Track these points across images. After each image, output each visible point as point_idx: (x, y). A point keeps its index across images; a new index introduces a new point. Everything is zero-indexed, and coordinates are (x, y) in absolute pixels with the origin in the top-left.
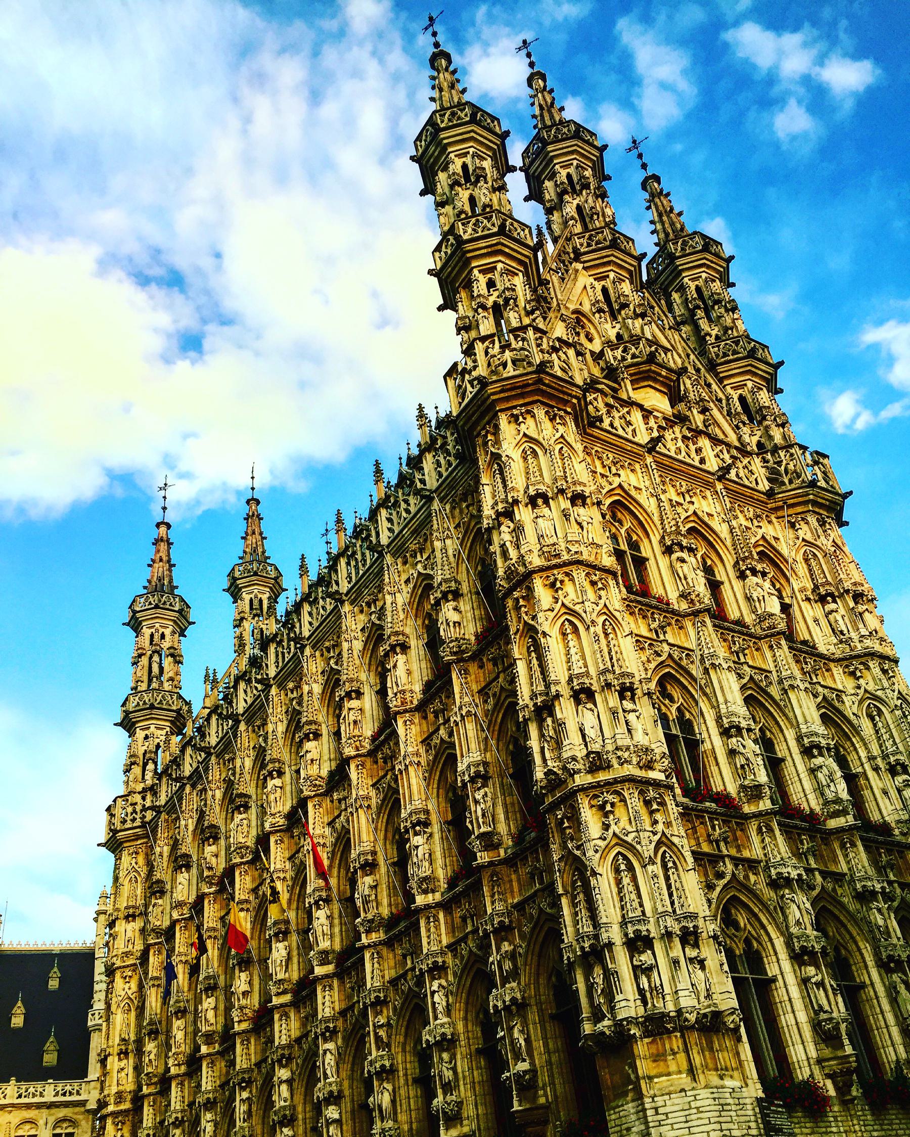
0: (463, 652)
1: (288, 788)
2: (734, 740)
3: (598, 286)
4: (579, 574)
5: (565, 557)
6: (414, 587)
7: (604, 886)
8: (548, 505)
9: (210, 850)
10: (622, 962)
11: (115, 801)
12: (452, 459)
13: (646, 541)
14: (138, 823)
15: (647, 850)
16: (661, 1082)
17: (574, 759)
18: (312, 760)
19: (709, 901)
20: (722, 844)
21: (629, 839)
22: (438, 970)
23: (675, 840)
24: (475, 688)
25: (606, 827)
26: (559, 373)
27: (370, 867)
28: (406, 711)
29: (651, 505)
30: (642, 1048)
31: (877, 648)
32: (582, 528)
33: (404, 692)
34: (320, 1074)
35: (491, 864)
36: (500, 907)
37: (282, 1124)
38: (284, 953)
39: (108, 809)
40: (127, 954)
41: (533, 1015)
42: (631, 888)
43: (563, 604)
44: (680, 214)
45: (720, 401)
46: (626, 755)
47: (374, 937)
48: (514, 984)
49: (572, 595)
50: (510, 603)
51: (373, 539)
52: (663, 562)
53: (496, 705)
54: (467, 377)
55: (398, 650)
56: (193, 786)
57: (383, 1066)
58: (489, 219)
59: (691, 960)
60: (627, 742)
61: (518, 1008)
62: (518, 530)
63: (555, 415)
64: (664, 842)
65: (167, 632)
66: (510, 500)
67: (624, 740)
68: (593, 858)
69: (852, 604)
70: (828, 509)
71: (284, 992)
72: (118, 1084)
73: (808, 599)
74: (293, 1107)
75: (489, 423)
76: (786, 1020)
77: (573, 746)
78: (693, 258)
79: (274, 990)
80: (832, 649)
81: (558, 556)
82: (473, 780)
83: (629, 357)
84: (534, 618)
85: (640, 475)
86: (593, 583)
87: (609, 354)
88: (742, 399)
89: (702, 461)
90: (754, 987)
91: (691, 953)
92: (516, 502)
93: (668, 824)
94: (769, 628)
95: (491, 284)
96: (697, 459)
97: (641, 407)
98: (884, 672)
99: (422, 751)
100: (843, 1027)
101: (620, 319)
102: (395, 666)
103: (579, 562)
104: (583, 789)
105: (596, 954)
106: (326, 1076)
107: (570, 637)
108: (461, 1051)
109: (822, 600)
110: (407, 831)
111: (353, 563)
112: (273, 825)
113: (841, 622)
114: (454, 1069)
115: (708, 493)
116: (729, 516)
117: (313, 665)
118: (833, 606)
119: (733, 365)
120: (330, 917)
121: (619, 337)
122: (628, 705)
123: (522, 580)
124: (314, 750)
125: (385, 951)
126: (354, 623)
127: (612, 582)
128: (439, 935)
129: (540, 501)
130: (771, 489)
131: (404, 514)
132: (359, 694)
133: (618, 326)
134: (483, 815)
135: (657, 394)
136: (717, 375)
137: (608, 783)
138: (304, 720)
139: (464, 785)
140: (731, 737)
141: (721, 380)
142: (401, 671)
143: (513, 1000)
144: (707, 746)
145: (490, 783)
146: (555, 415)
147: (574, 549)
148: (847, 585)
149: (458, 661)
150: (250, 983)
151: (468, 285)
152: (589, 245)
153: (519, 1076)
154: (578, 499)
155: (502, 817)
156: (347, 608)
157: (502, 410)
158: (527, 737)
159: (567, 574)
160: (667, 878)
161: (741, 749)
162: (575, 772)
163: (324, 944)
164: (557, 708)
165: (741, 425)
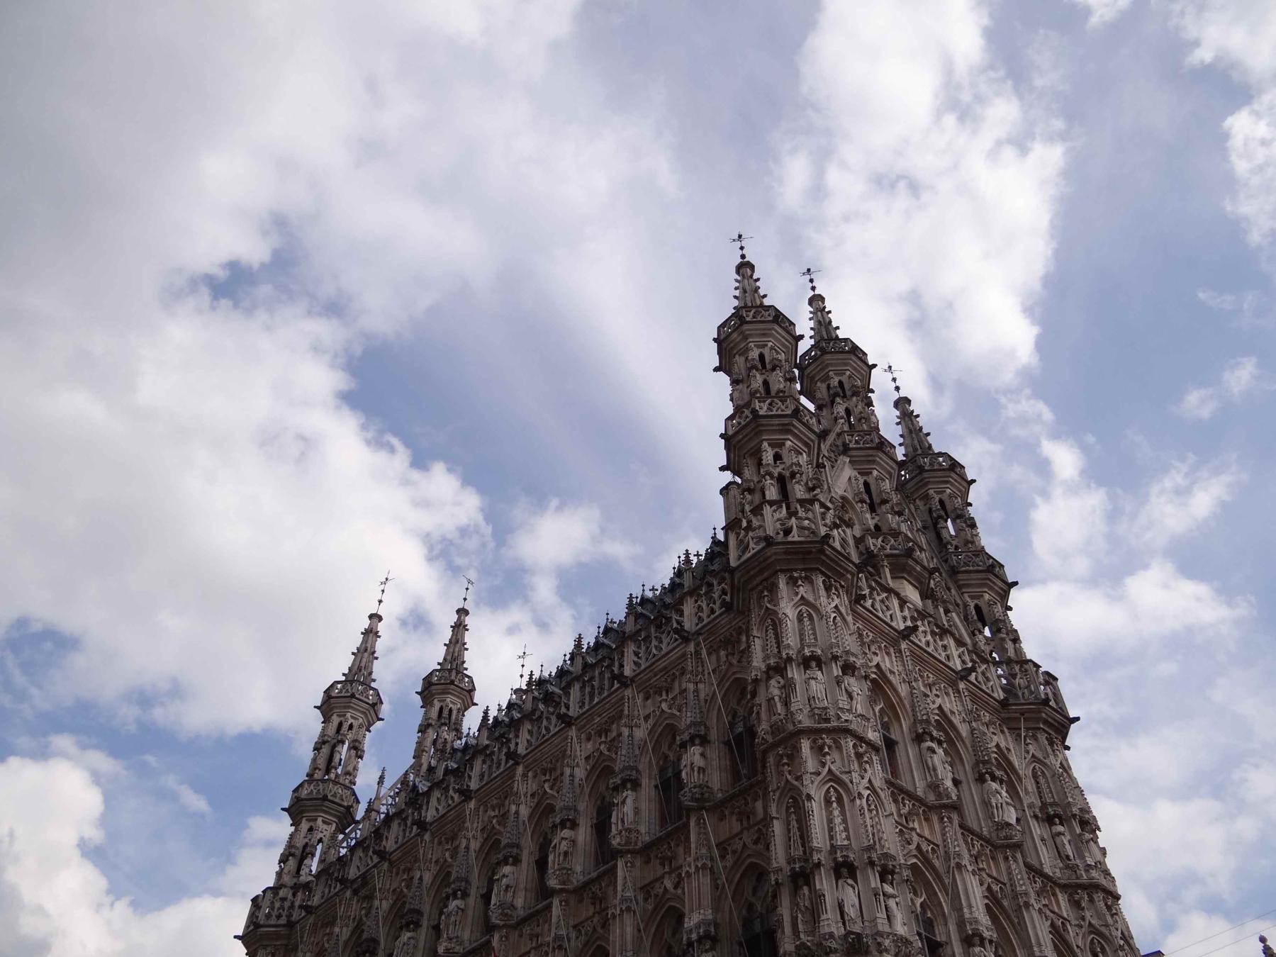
1: (470, 913)
2: (977, 949)
3: (861, 481)
4: (849, 743)
5: (834, 724)
6: (655, 725)
8: (821, 669)
11: (264, 892)
12: (716, 607)
13: (896, 725)
14: (283, 921)
17: (831, 935)
18: (507, 887)
26: (839, 548)
28: (628, 852)
29: (903, 690)
31: (1104, 882)
33: (629, 830)
43: (830, 770)
44: (928, 434)
45: (958, 605)
46: (887, 942)
49: (838, 763)
50: (771, 760)
51: (616, 669)
52: (912, 751)
53: (735, 863)
54: (751, 534)
55: (629, 786)
56: (355, 892)
58: (783, 402)
60: (887, 929)
62: (788, 687)
63: (831, 585)
66: (784, 656)
69: (1078, 831)
70: (1057, 731)
73: (1036, 817)
78: (940, 474)
80: (1058, 874)
81: (827, 720)
82: (700, 940)
84: (799, 778)
86: (859, 756)
88: (977, 608)
92: (789, 659)
94: (1006, 838)
95: (777, 457)
97: (898, 595)
98: (1109, 908)
99: (640, 897)
101: (879, 511)
102: (624, 802)
103: (847, 731)
107: (835, 805)
109: (1049, 820)
111: (588, 689)
113: (1067, 846)
115: (950, 691)
116: (972, 716)
117: (524, 785)
118: (1060, 828)
119: (974, 576)
121: (877, 527)
123: (788, 738)
124: (511, 876)
126: (581, 749)
129: (814, 664)
130: (1006, 699)
131: (654, 651)
132: (574, 825)
136: (956, 582)
138: (504, 841)
139: (690, 944)
140: (974, 945)
141: (959, 587)
142: (628, 808)
146: (831, 585)
147: (844, 717)
148: (1075, 810)
151: (757, 454)
154: (848, 669)
156: (573, 732)
157: (782, 571)
159: (835, 741)
162: (831, 951)
164: (817, 877)
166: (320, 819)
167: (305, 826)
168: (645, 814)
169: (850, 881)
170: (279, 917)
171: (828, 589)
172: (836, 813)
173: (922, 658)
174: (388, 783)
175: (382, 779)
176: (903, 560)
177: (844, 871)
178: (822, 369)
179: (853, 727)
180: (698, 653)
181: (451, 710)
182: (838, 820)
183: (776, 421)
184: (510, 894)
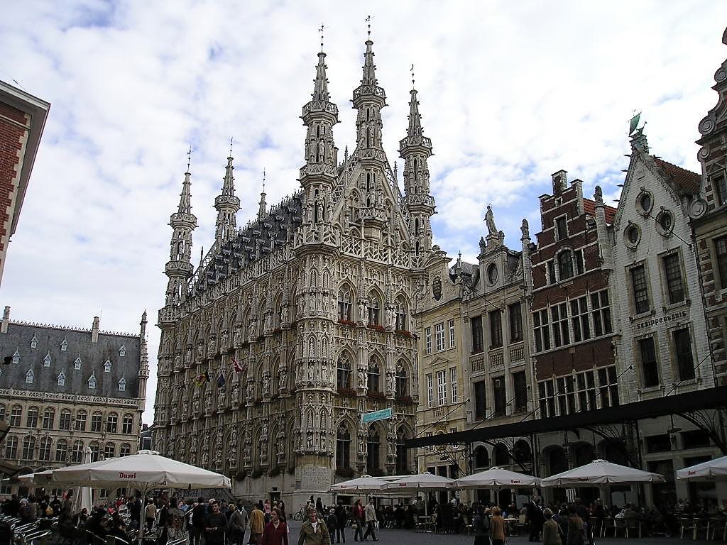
10: (304, 437)
14: (171, 321)
15: (317, 410)
19: (335, 422)
27: (252, 382)
34: (231, 438)
35: (283, 398)
40: (166, 373)
61: (284, 438)
67: (319, 379)
77: (305, 379)
88: (417, 220)
89: (386, 259)
93: (327, 403)
95: (317, 192)
163: (236, 401)
167: (173, 280)
169: (312, 367)
170: (169, 319)
173: (371, 266)
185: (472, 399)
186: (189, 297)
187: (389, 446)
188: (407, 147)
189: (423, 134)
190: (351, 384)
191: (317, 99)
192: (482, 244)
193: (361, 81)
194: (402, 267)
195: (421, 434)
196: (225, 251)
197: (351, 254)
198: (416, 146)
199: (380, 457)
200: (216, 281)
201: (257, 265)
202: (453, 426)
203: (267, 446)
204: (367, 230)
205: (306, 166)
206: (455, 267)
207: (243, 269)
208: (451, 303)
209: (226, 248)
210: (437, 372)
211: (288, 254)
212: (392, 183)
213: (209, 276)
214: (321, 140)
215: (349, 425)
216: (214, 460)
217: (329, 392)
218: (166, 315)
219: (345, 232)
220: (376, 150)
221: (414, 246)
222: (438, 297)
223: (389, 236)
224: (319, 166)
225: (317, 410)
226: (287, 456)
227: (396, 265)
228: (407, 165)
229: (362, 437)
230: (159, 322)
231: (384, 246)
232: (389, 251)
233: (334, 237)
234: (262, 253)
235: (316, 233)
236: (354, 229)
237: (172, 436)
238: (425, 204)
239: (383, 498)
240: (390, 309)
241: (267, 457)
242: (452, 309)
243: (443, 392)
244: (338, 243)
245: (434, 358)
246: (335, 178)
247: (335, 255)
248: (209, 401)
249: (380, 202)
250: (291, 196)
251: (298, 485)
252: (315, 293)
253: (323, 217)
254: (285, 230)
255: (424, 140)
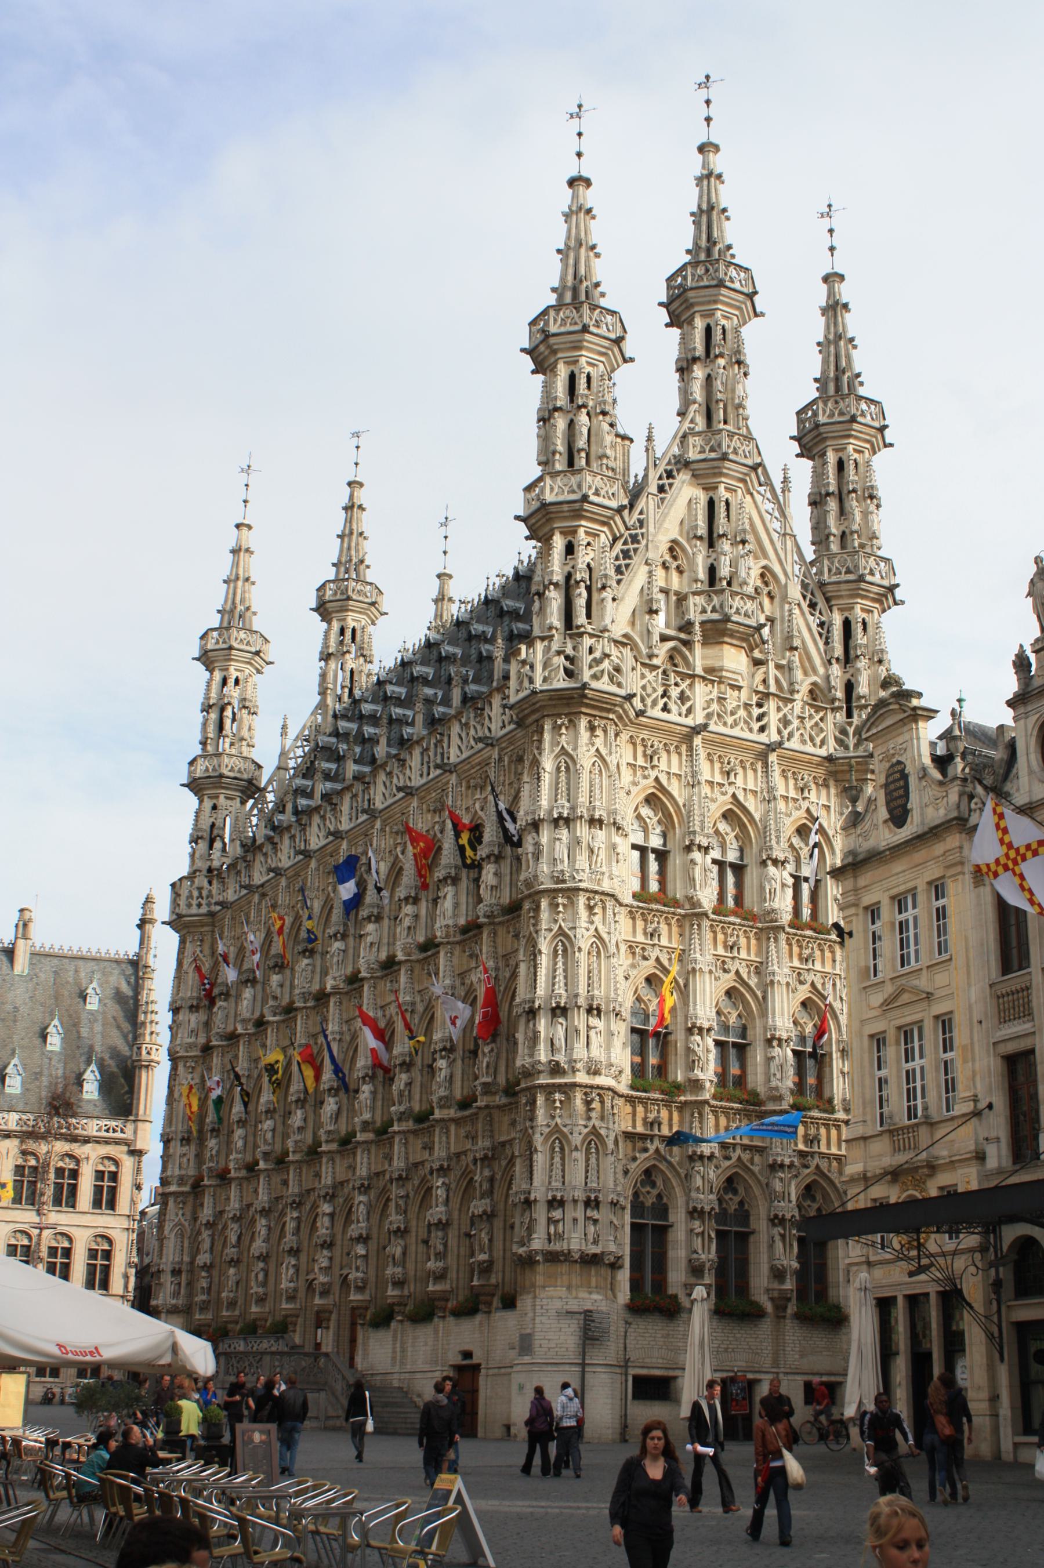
0: (495, 917)
5: (569, 885)
7: (540, 1160)
9: (275, 978)
10: (541, 1214)
11: (180, 880)
14: (204, 910)
15: (576, 1139)
16: (550, 1291)
19: (626, 1172)
20: (656, 1126)
21: (565, 1130)
22: (442, 1171)
23: (603, 1132)
24: (501, 951)
25: (553, 1117)
27: (407, 1066)
28: (448, 943)
30: (541, 1268)
32: (592, 851)
34: (354, 1218)
35: (487, 1107)
36: (487, 1143)
37: (322, 1246)
38: (335, 1107)
39: (173, 885)
40: (190, 1046)
41: (498, 1223)
42: (559, 1166)
47: (405, 1126)
48: (488, 1201)
57: (399, 1228)
59: (589, 1218)
61: (489, 1216)
62: (537, 844)
64: (594, 1131)
65: (241, 678)
68: (538, 1140)
71: (332, 1141)
72: (180, 1168)
74: (333, 1236)
75: (537, 721)
76: (671, 1254)
77: (543, 1055)
79: (323, 1138)
81: (564, 881)
83: (709, 609)
84: (537, 932)
85: (684, 758)
87: (692, 600)
88: (847, 624)
89: (762, 729)
90: (650, 1234)
91: (589, 1213)
95: (570, 549)
96: (756, 726)
99: (458, 983)
100: (708, 1265)
104: (541, 1086)
105: (528, 1203)
106: (358, 1222)
108: (452, 1233)
110: (435, 1052)
112: (333, 987)
114: (445, 1245)
119: (844, 586)
120: (374, 1093)
122: (594, 1021)
125: (411, 1138)
127: (610, 903)
128: (448, 1143)
129: (561, 823)
133: (714, 556)
134: (488, 1066)
135: (733, 650)
137: (560, 1085)
141: (828, 600)
143: (485, 1212)
144: (672, 1038)
145: (498, 1040)
147: (578, 878)
149: (490, 924)
150: (305, 1120)
152: (702, 451)
153: (480, 1263)
155: (502, 1069)
156: (415, 803)
158: (516, 1030)
159: (568, 898)
160: (587, 1160)
161: (697, 1049)
163: (367, 1116)
165: (834, 661)
166: (222, 797)
167: (208, 804)
168: (463, 907)
170: (199, 905)
171: (592, 728)
172: (560, 964)
174: (293, 732)
175: (284, 727)
176: (721, 626)
177: (558, 1012)
178: (688, 308)
179: (582, 885)
180: (500, 759)
181: (354, 630)
182: (560, 971)
183: (565, 507)
184: (375, 949)
185: (1000, 1102)
186: (251, 847)
187: (777, 1238)
188: (817, 426)
189: (862, 391)
190: (671, 1068)
191: (568, 297)
192: (1021, 664)
193: (688, 252)
194: (809, 748)
195: (859, 1200)
196: (343, 725)
197: (665, 716)
198: (835, 424)
199: (752, 1268)
200: (317, 800)
201: (417, 752)
202: (944, 1179)
203: (446, 1235)
204: (712, 651)
205: (541, 479)
206: (947, 736)
207: (383, 766)
208: (933, 834)
209: (344, 717)
210: (899, 1028)
211: (497, 720)
212: (777, 525)
213: (301, 792)
214: (580, 407)
215: (666, 1180)
216: (311, 1277)
217: (609, 1089)
218: (190, 896)
219: (651, 656)
220: (731, 435)
221: (840, 694)
222: (899, 816)
223: (771, 665)
224: (574, 480)
225: (576, 1139)
226: (498, 1266)
227: (794, 744)
228: (818, 475)
229: (702, 1212)
230: (173, 912)
231: (757, 692)
232: (772, 705)
233: (618, 669)
234: (432, 722)
235: (567, 658)
236: (674, 649)
237: (207, 1213)
238: (869, 578)
239: (759, 1381)
240: (775, 862)
241: (445, 1269)
242: (939, 849)
243: (918, 1084)
244: (633, 682)
245: (889, 989)
246: (620, 510)
247: (620, 717)
248: (297, 1118)
249: (743, 574)
250: (510, 573)
251: (525, 1344)
252: (568, 821)
253: (589, 616)
254: (490, 659)
255: (864, 406)
